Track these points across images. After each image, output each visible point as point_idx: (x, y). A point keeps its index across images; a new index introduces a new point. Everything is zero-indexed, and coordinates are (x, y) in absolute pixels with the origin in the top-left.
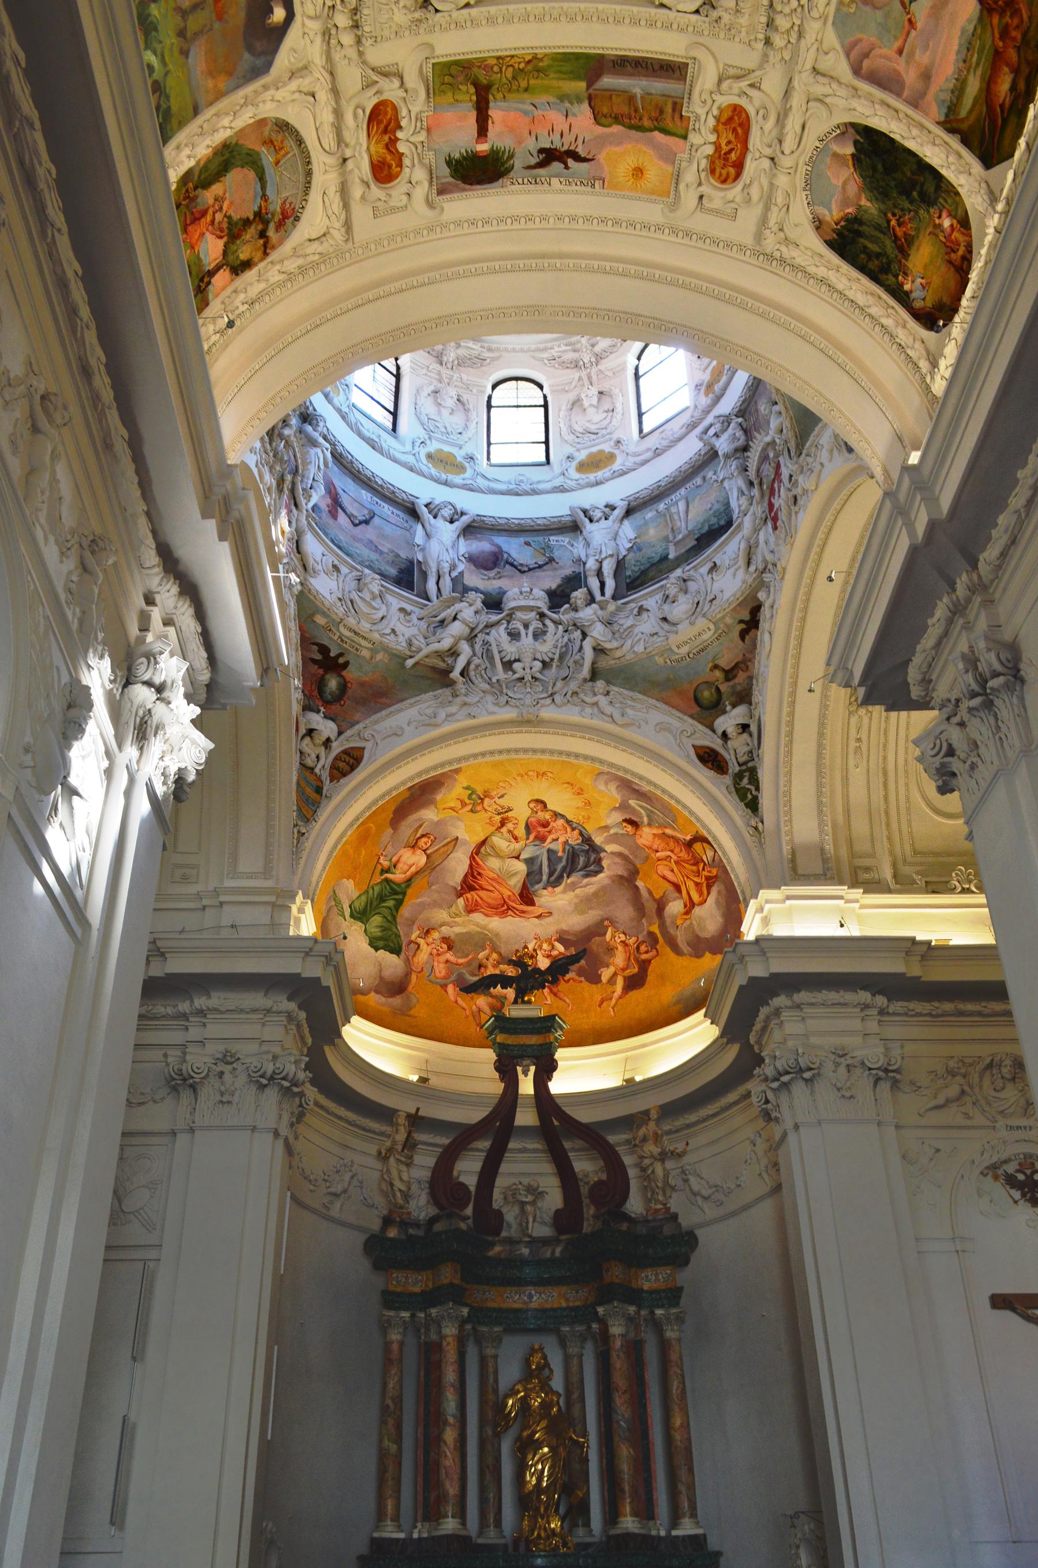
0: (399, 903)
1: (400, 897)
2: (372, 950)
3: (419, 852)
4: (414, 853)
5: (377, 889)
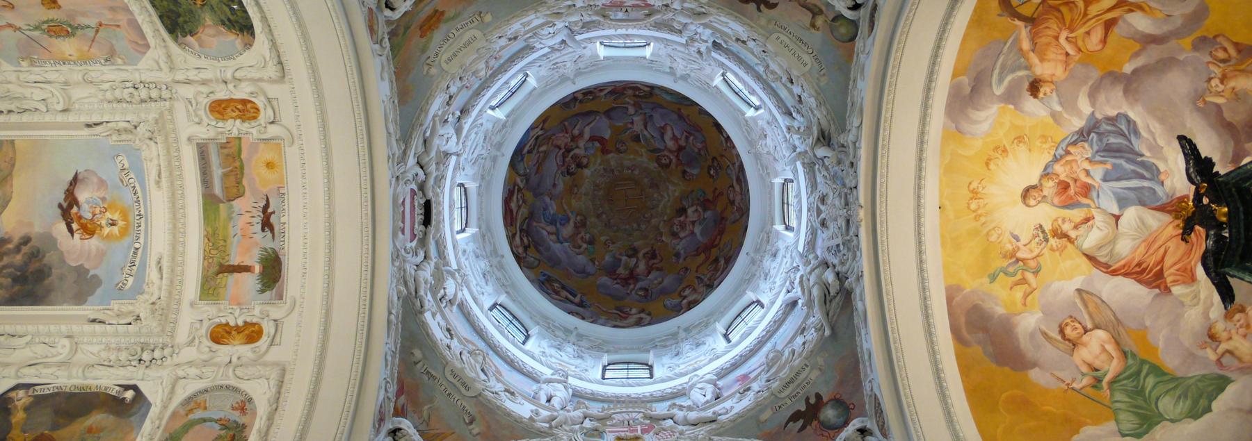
0: (1157, 370)
1: (1146, 368)
2: (1207, 417)
3: (1085, 338)
4: (1084, 345)
5: (1119, 396)
